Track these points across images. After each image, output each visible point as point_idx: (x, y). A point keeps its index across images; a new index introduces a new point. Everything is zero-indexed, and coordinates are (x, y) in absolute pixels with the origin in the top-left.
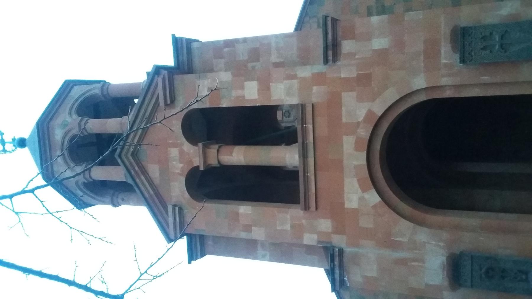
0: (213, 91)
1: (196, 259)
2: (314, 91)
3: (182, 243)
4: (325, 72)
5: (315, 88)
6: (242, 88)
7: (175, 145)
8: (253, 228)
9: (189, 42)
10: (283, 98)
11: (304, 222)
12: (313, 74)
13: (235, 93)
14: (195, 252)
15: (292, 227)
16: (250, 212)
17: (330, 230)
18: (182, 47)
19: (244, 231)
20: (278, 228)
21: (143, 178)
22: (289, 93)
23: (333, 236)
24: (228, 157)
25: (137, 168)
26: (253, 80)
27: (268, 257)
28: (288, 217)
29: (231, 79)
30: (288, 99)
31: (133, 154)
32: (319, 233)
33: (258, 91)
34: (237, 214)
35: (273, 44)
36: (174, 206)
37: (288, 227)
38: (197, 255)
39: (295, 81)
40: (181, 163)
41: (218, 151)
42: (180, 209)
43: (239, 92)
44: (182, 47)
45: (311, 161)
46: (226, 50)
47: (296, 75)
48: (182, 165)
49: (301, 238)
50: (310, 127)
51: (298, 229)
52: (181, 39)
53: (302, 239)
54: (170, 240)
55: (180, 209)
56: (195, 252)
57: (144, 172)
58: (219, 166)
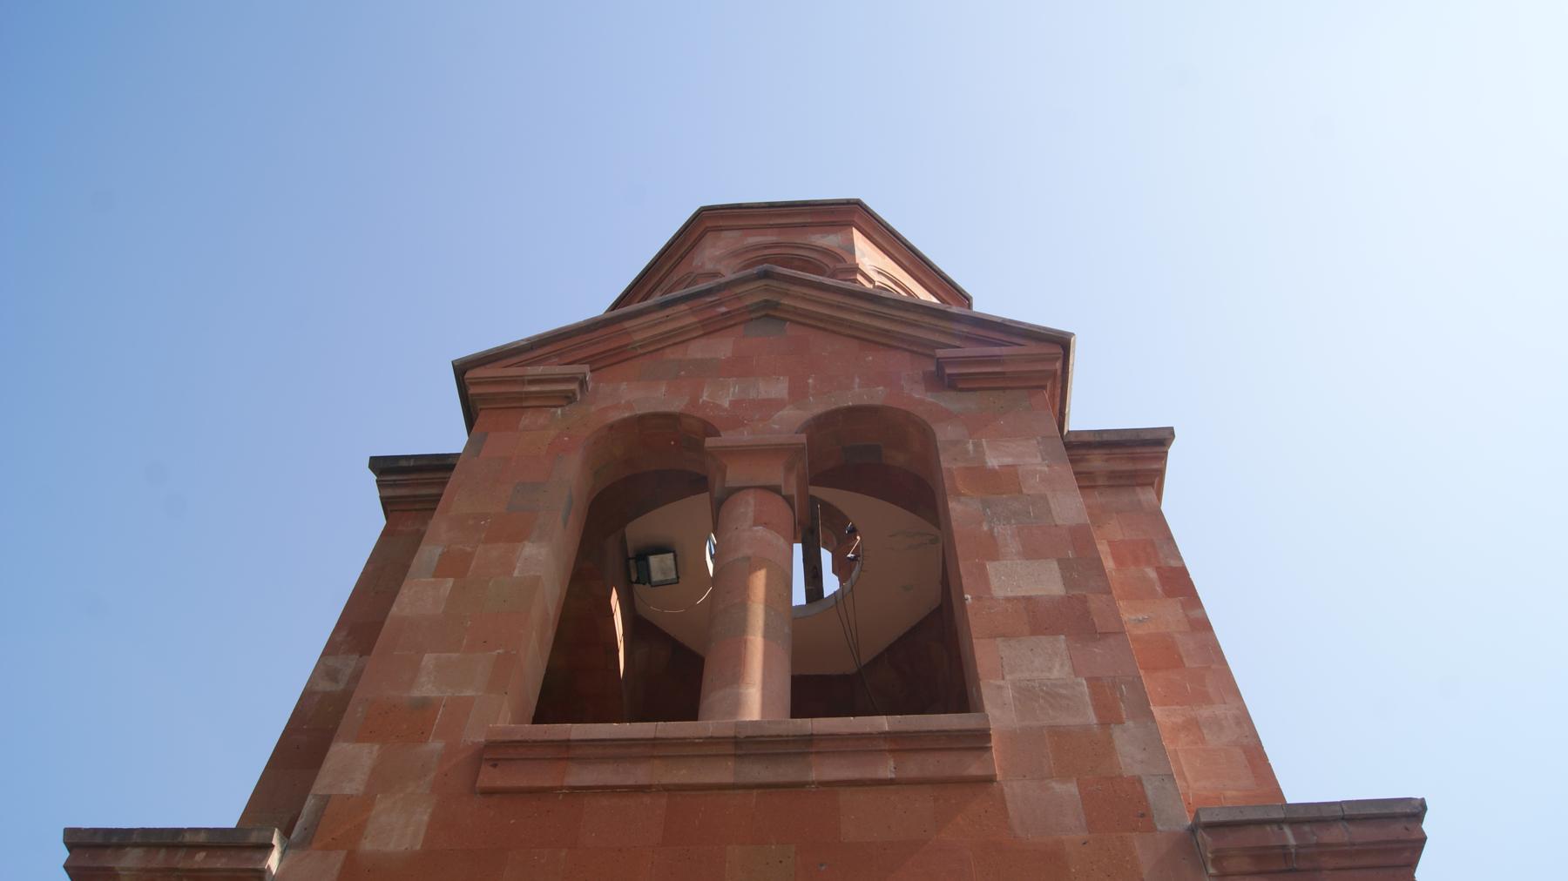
0: (1002, 483)
1: (381, 484)
2: (1058, 787)
3: (444, 431)
4: (1152, 828)
5: (1069, 789)
6: (1031, 553)
7: (798, 394)
8: (450, 582)
9: (1154, 479)
10: (1008, 677)
11: (436, 745)
12: (1137, 781)
13: (1005, 532)
14: (409, 484)
15: (425, 705)
16: (516, 573)
17: (367, 846)
18: (1135, 458)
19: (442, 555)
20: (429, 659)
21: (693, 319)
22: (1026, 694)
23: (337, 858)
24: (751, 515)
25: (723, 309)
26: (1067, 581)
27: (325, 686)
28: (469, 693)
29: (1059, 522)
30: (1009, 693)
31: (767, 304)
32: (366, 802)
33: (1028, 599)
34: (519, 536)
35: (1205, 712)
36: (583, 383)
37: (426, 688)
38: (394, 485)
39: (1092, 718)
40: (734, 404)
41: (775, 490)
42: (569, 398)
43: (1014, 546)
44: (1135, 458)
45: (723, 773)
46: (1152, 574)
47: (1121, 722)
48: (726, 405)
49: (365, 735)
50: (887, 770)
51: (404, 724)
53: (359, 739)
54: (462, 370)
55: (569, 398)
56: (409, 484)
57: (711, 328)
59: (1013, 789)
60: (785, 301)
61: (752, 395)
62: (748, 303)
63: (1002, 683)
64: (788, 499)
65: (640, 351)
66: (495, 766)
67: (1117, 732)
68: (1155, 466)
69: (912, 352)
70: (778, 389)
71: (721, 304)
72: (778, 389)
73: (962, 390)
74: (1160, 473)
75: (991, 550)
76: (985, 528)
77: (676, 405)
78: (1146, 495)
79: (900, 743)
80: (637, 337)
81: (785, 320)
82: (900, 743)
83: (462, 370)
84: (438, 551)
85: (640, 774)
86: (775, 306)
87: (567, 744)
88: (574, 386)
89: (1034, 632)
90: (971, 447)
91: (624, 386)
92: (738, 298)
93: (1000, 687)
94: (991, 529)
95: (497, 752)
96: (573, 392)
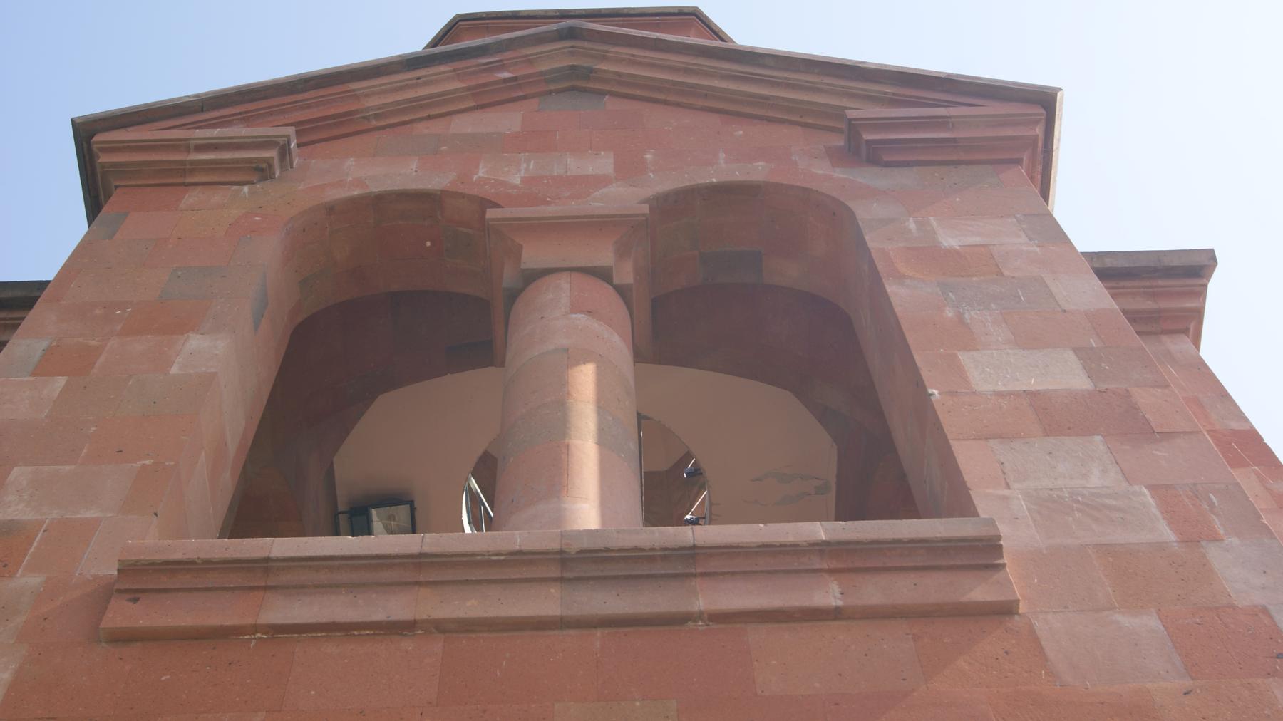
5: (1149, 622)
6: (1028, 340)
8: (61, 381)
10: (1015, 486)
11: (28, 580)
16: (174, 370)
18: (1163, 290)
25: (506, 75)
31: (574, 71)
34: (182, 325)
36: (284, 152)
39: (1167, 534)
41: (603, 274)
44: (1163, 290)
48: (517, 180)
50: (829, 595)
52: (1201, 293)
54: (87, 133)
55: (262, 172)
58: (508, 277)
59: (1050, 624)
60: (603, 66)
61: (557, 170)
62: (544, 67)
63: (1006, 492)
64: (622, 291)
65: (374, 123)
66: (136, 600)
67: (1213, 553)
68: (1190, 304)
69: (805, 125)
70: (603, 164)
71: (502, 67)
72: (603, 164)
73: (889, 165)
74: (1198, 314)
75: (966, 338)
76: (949, 313)
77: (436, 182)
78: (1178, 345)
79: (843, 559)
80: (372, 102)
81: (602, 93)
82: (843, 559)
83: (87, 133)
84: (44, 344)
85: (396, 607)
86: (588, 74)
87: (266, 565)
88: (272, 154)
89: (1047, 433)
90: (912, 225)
91: (350, 161)
92: (529, 61)
93: (1005, 498)
94: (960, 319)
95: (140, 578)
96: (269, 162)
